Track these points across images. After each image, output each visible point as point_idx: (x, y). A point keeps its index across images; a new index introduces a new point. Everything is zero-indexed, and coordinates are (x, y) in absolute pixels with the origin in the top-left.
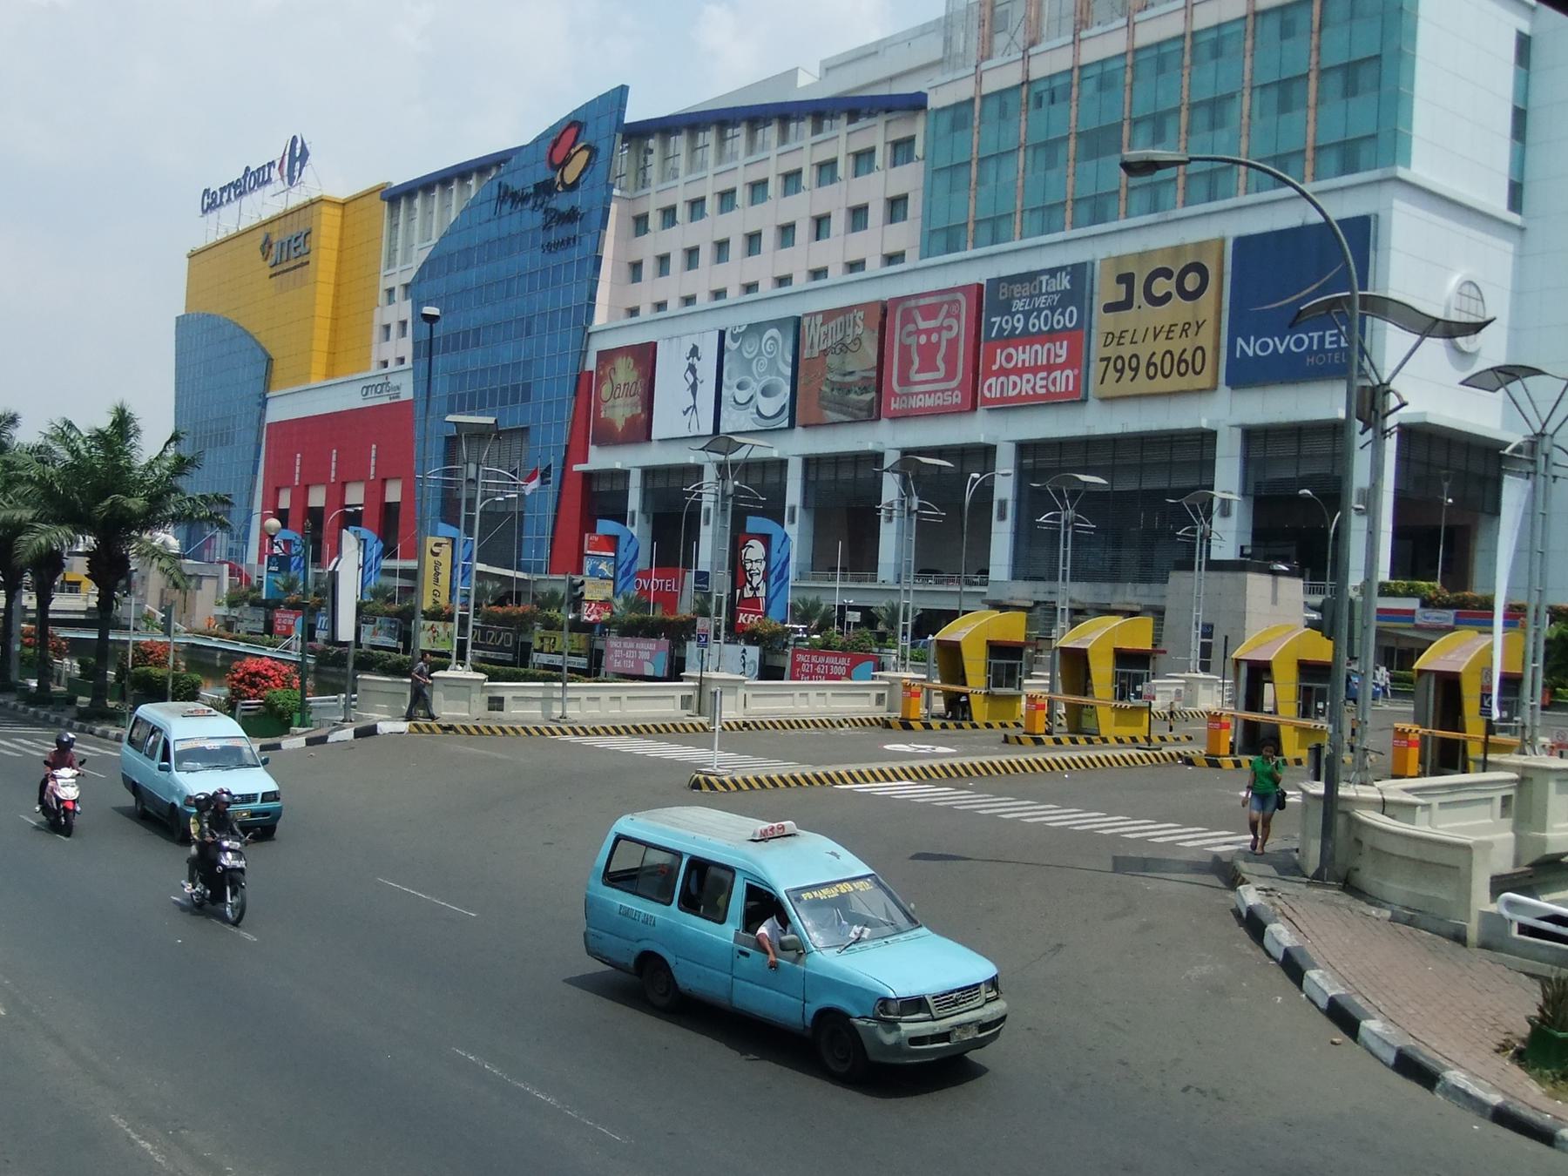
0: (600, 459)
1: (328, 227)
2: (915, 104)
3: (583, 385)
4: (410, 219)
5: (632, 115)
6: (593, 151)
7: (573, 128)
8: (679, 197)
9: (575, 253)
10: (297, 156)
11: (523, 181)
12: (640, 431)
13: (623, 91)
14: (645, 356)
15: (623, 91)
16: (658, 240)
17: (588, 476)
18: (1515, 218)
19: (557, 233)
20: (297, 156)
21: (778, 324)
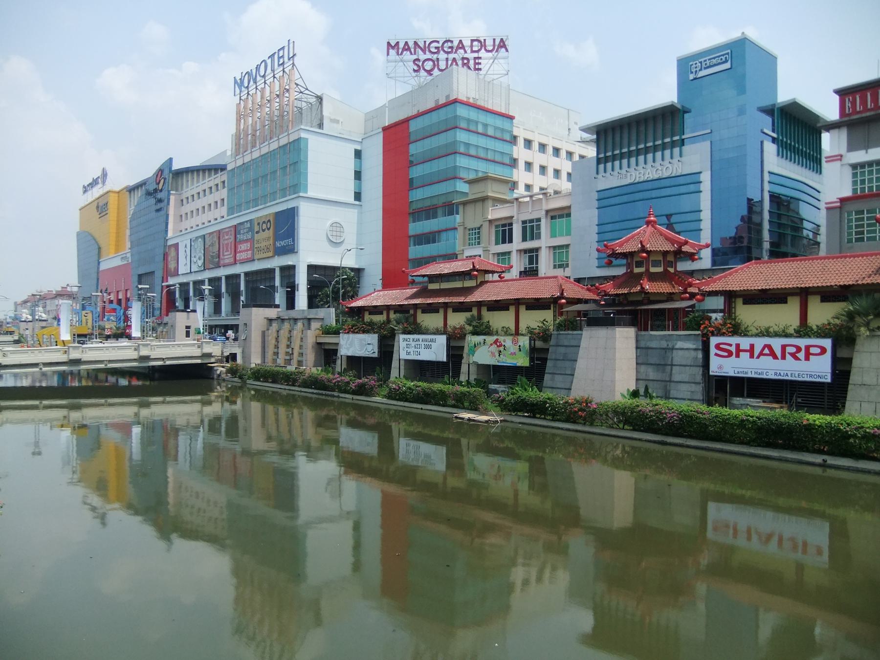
0: (171, 281)
1: (113, 200)
2: (223, 168)
3: (165, 256)
5: (176, 166)
6: (165, 179)
7: (161, 171)
8: (189, 194)
9: (162, 213)
10: (104, 174)
11: (151, 188)
12: (176, 274)
13: (171, 159)
14: (176, 246)
15: (171, 159)
16: (188, 208)
17: (168, 286)
18: (357, 203)
19: (159, 206)
20: (104, 174)
21: (200, 237)
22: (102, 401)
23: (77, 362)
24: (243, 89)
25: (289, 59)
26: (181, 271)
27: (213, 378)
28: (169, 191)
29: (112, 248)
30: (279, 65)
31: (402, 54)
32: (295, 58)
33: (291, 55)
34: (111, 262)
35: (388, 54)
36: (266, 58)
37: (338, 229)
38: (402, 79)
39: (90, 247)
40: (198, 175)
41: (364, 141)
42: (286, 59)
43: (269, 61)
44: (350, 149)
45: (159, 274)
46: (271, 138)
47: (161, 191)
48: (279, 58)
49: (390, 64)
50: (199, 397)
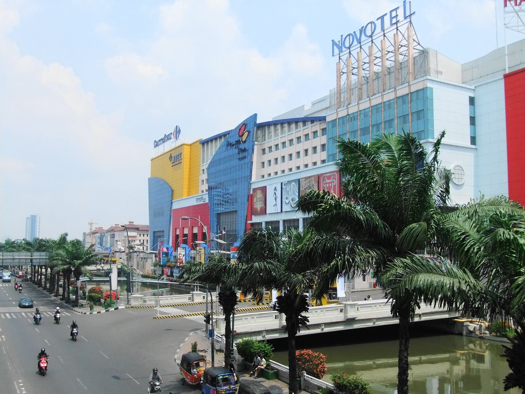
0: (255, 219)
1: (186, 152)
2: (322, 119)
3: (250, 198)
4: (208, 149)
5: (259, 121)
6: (249, 132)
7: (244, 125)
8: (272, 144)
9: (246, 160)
10: (178, 131)
11: (233, 140)
12: (264, 211)
13: (256, 115)
14: (264, 190)
15: (256, 115)
16: (270, 156)
17: (252, 224)
18: (473, 146)
19: (241, 155)
20: (178, 131)
21: (294, 181)
22: (370, 362)
23: (352, 321)
24: (344, 49)
25: (405, 18)
26: (270, 209)
27: (461, 334)
28: (253, 142)
29: (185, 191)
30: (392, 24)
31: (520, 4)
32: (412, 17)
33: (408, 14)
34: (184, 201)
35: (505, 5)
36: (374, 20)
37: (460, 172)
38: (516, 28)
39: (160, 191)
40: (282, 127)
41: (477, 89)
42: (401, 17)
43: (378, 23)
44: (465, 97)
45: (243, 212)
46: (384, 91)
47: (245, 142)
48: (391, 18)
49: (506, 15)
50: (447, 355)
